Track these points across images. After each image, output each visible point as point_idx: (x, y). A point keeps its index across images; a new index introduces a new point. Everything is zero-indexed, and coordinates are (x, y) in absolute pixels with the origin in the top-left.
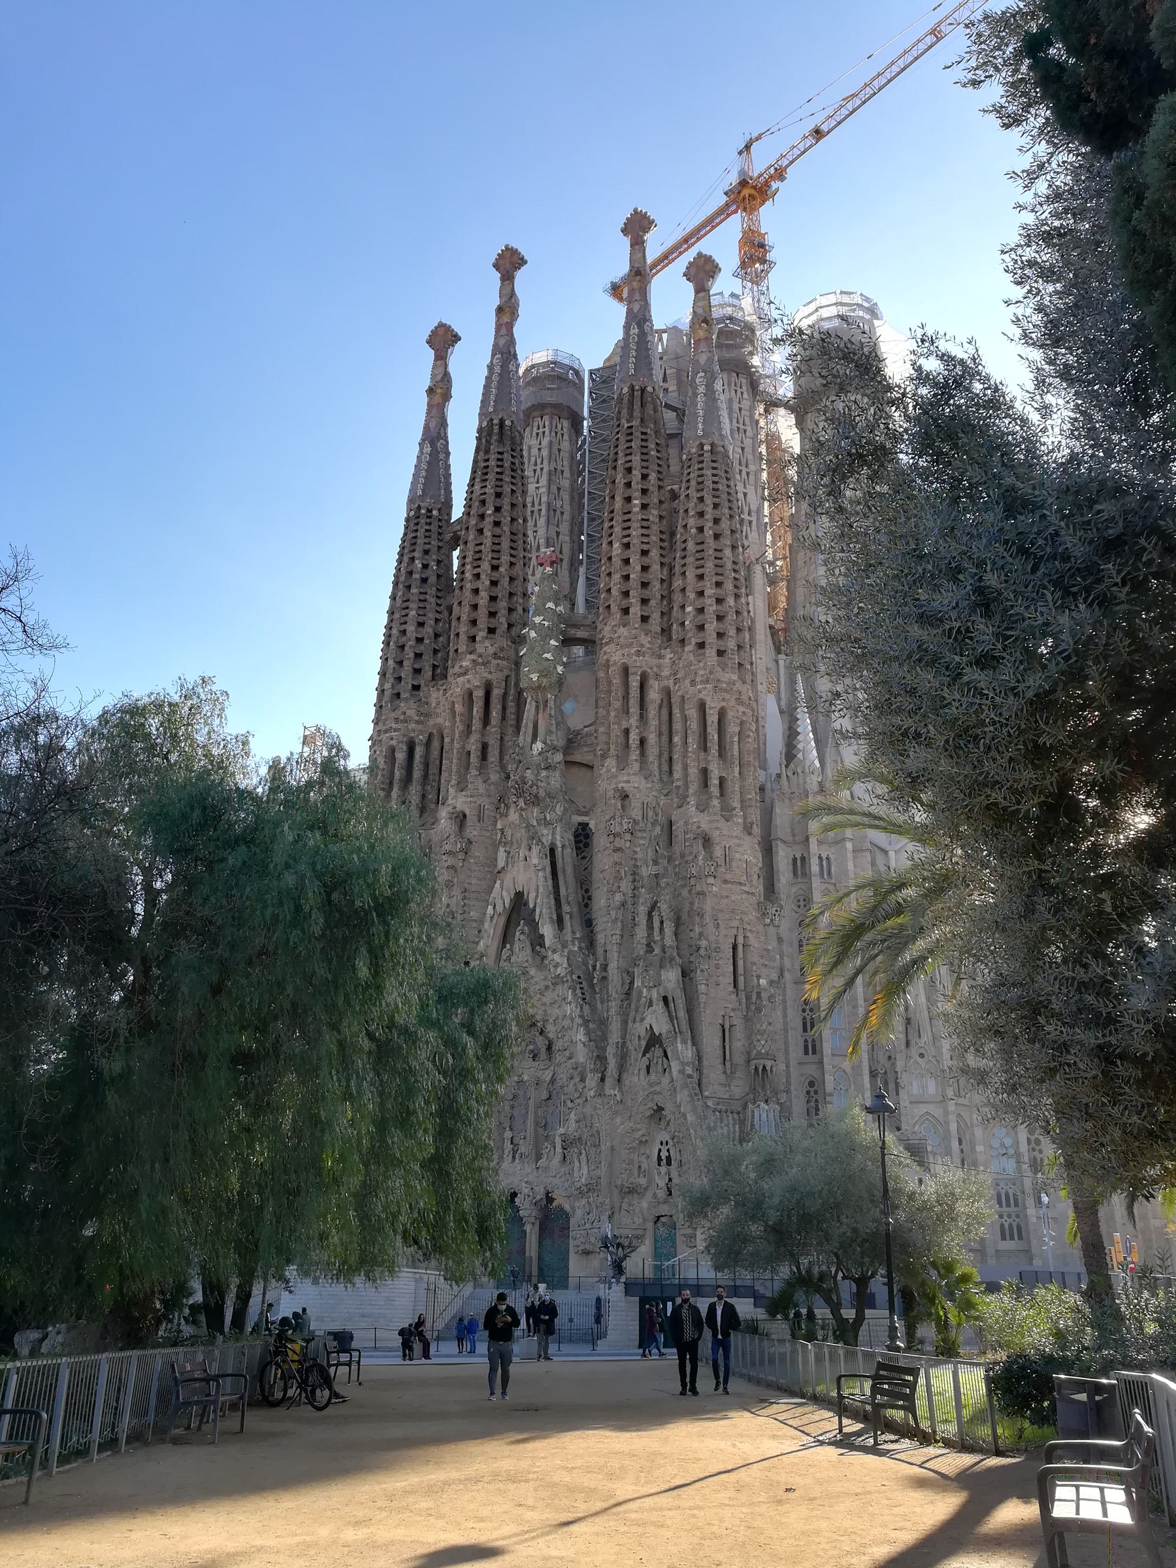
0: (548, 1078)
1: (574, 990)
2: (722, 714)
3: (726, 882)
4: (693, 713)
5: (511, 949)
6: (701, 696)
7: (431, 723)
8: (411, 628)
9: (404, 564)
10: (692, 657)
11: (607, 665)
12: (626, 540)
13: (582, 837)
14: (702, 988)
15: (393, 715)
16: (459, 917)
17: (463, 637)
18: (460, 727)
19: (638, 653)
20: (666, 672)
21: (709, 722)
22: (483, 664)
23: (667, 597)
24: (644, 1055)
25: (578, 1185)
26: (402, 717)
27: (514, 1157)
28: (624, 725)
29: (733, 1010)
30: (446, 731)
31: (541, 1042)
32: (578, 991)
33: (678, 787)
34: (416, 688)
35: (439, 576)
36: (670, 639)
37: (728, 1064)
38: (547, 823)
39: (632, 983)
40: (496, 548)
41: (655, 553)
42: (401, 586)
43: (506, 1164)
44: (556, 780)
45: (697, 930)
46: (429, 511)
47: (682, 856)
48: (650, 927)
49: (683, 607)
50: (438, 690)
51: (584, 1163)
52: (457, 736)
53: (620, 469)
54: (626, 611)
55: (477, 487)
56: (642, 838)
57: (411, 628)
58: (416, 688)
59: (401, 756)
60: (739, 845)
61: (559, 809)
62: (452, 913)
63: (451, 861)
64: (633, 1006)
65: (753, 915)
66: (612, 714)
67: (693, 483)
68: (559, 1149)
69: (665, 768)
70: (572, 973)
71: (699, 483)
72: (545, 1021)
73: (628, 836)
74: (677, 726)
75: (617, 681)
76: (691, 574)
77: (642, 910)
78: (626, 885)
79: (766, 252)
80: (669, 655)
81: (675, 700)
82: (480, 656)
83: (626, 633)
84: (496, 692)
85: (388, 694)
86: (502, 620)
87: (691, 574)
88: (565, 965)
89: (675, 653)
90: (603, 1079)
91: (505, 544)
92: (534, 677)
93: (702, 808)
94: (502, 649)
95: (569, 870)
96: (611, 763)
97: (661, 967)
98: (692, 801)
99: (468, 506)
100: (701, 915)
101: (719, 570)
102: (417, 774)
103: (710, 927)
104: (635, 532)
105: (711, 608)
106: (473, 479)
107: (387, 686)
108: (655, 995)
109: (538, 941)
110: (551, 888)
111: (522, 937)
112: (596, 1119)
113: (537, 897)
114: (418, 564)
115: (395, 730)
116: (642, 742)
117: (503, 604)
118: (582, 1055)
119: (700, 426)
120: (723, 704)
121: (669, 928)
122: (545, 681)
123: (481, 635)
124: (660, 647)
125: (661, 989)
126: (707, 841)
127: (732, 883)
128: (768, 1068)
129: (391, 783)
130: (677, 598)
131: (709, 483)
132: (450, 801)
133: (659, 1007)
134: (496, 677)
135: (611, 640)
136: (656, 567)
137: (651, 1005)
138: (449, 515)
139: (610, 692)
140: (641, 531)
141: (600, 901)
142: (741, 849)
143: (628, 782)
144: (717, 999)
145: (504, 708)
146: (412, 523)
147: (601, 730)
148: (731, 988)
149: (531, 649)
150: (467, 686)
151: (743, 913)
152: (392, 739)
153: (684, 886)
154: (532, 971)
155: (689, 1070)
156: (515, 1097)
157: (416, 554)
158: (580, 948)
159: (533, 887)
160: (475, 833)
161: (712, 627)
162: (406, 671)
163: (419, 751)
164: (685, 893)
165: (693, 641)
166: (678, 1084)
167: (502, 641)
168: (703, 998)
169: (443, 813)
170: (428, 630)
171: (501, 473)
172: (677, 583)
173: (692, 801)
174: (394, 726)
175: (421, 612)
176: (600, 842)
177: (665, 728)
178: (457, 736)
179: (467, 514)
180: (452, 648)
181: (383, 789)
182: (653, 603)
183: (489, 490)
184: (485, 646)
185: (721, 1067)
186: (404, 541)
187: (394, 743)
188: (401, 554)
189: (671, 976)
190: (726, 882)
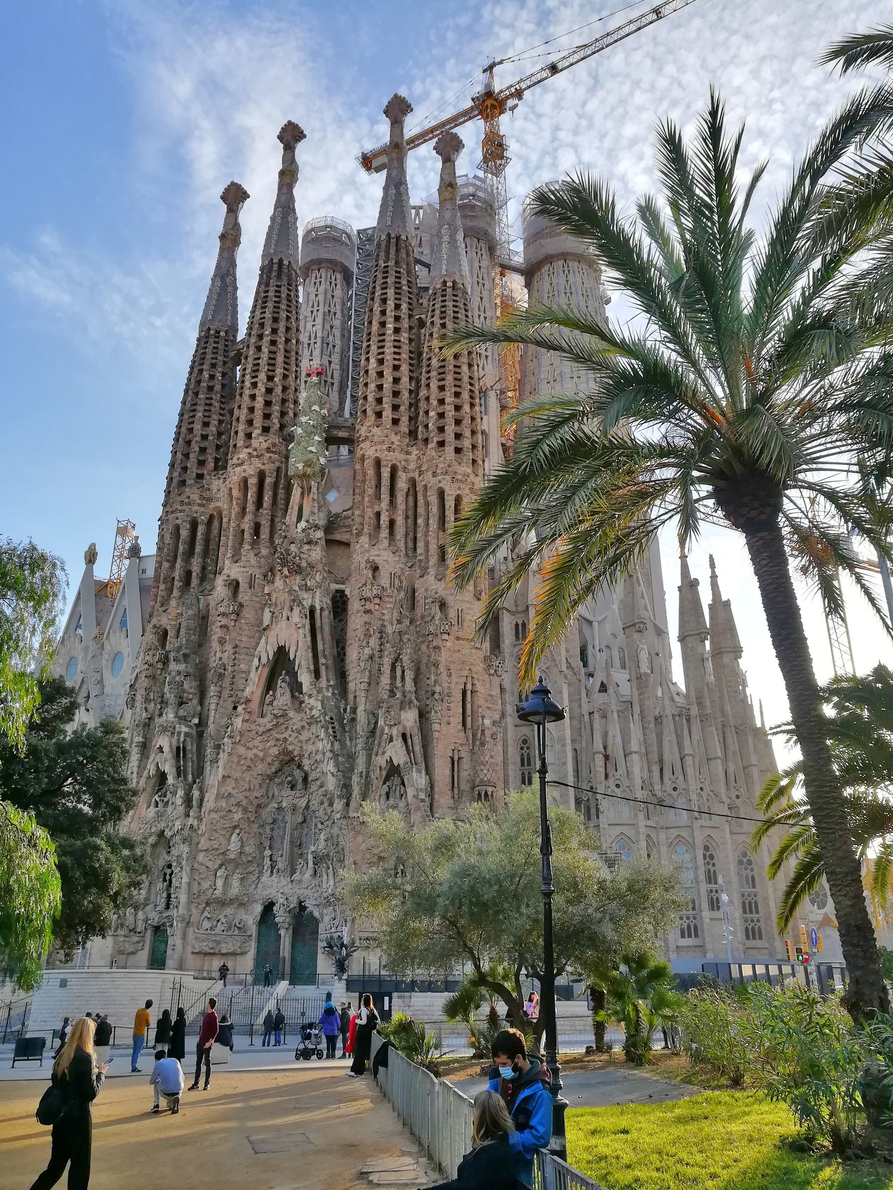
0: (304, 805)
1: (327, 729)
2: (458, 500)
3: (458, 638)
4: (433, 499)
5: (274, 695)
6: (441, 485)
7: (212, 505)
8: (197, 427)
9: (194, 375)
10: (434, 453)
11: (363, 458)
12: (380, 357)
13: (339, 603)
14: (436, 727)
15: (179, 498)
16: (230, 669)
17: (241, 434)
18: (236, 509)
19: (389, 449)
20: (412, 466)
21: (447, 507)
22: (257, 456)
23: (414, 405)
24: (384, 783)
25: (325, 895)
27: (272, 872)
28: (377, 509)
29: (461, 745)
30: (224, 513)
31: (298, 774)
32: (330, 731)
33: (420, 561)
35: (223, 386)
36: (416, 438)
37: (456, 790)
38: (308, 589)
39: (376, 723)
40: (272, 362)
41: (405, 368)
42: (190, 393)
43: (265, 878)
44: (317, 554)
45: (433, 678)
46: (218, 332)
47: (423, 617)
48: (393, 677)
49: (427, 413)
51: (331, 876)
52: (233, 516)
53: (377, 299)
54: (379, 415)
55: (258, 313)
56: (389, 602)
57: (197, 427)
58: (200, 476)
59: (184, 533)
60: (470, 609)
61: (318, 577)
62: (224, 665)
63: (224, 621)
64: (376, 742)
65: (480, 667)
66: (366, 499)
67: (437, 312)
68: (311, 864)
69: (411, 545)
70: (325, 714)
71: (442, 312)
72: (301, 756)
73: (377, 601)
74: (421, 510)
75: (371, 472)
76: (434, 385)
77: (387, 661)
78: (374, 642)
79: (504, 150)
80: (415, 452)
81: (419, 488)
82: (255, 450)
83: (379, 433)
84: (269, 480)
85: (175, 481)
86: (275, 421)
87: (434, 385)
88: (320, 708)
90: (348, 804)
91: (280, 359)
93: (440, 578)
94: (274, 445)
95: (327, 628)
96: (364, 540)
97: (401, 709)
98: (432, 571)
99: (250, 328)
100: (436, 665)
101: (458, 383)
102: (198, 548)
103: (444, 676)
104: (389, 350)
105: (450, 413)
106: (255, 306)
107: (176, 474)
108: (395, 731)
109: (296, 687)
110: (309, 643)
111: (283, 685)
112: (341, 839)
113: (296, 651)
114: (206, 375)
115: (181, 511)
116: (392, 523)
117: (276, 408)
118: (331, 784)
119: (444, 267)
120: (459, 492)
121: (409, 675)
122: (309, 470)
123: (256, 432)
124: (408, 445)
125: (400, 727)
126: (443, 605)
127: (463, 639)
128: (489, 793)
129: (175, 557)
130: (423, 405)
131: (450, 313)
132: (225, 571)
133: (398, 743)
134: (269, 468)
136: (405, 380)
137: (391, 740)
138: (235, 337)
139: (364, 481)
140: (393, 350)
141: (352, 654)
142: (471, 612)
143: (379, 555)
144: (448, 734)
145: (275, 495)
146: (203, 340)
147: (357, 512)
148: (460, 727)
151: (472, 664)
153: (423, 642)
154: (291, 714)
155: (422, 796)
156: (275, 821)
158: (333, 694)
159: (294, 642)
160: (246, 598)
161: (450, 429)
162: (192, 463)
163: (201, 529)
164: (424, 647)
165: (435, 440)
166: (412, 807)
167: (274, 438)
168: (436, 735)
169: (220, 581)
170: (213, 429)
171: (278, 302)
172: (423, 393)
173: (432, 571)
174: (180, 508)
175: (207, 414)
176: (354, 606)
177: (410, 513)
178: (233, 516)
179: (249, 335)
180: (232, 443)
181: (168, 561)
182: (402, 408)
183: (268, 315)
184: (259, 442)
185: (450, 793)
186: (195, 356)
187: (179, 522)
188: (192, 368)
189: (410, 718)
190: (458, 638)
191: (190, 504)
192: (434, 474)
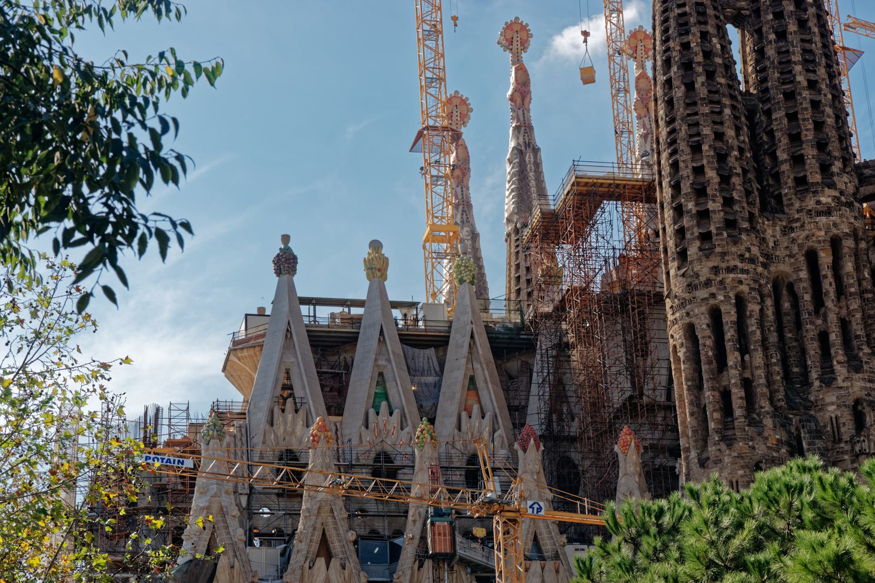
8: (731, 133)
26: (747, 255)
34: (751, 217)
50: (774, 225)
115: (743, 271)
150: (835, 231)
152: (740, 282)
157: (711, 29)
174: (740, 265)
187: (744, 288)
191: (752, 261)
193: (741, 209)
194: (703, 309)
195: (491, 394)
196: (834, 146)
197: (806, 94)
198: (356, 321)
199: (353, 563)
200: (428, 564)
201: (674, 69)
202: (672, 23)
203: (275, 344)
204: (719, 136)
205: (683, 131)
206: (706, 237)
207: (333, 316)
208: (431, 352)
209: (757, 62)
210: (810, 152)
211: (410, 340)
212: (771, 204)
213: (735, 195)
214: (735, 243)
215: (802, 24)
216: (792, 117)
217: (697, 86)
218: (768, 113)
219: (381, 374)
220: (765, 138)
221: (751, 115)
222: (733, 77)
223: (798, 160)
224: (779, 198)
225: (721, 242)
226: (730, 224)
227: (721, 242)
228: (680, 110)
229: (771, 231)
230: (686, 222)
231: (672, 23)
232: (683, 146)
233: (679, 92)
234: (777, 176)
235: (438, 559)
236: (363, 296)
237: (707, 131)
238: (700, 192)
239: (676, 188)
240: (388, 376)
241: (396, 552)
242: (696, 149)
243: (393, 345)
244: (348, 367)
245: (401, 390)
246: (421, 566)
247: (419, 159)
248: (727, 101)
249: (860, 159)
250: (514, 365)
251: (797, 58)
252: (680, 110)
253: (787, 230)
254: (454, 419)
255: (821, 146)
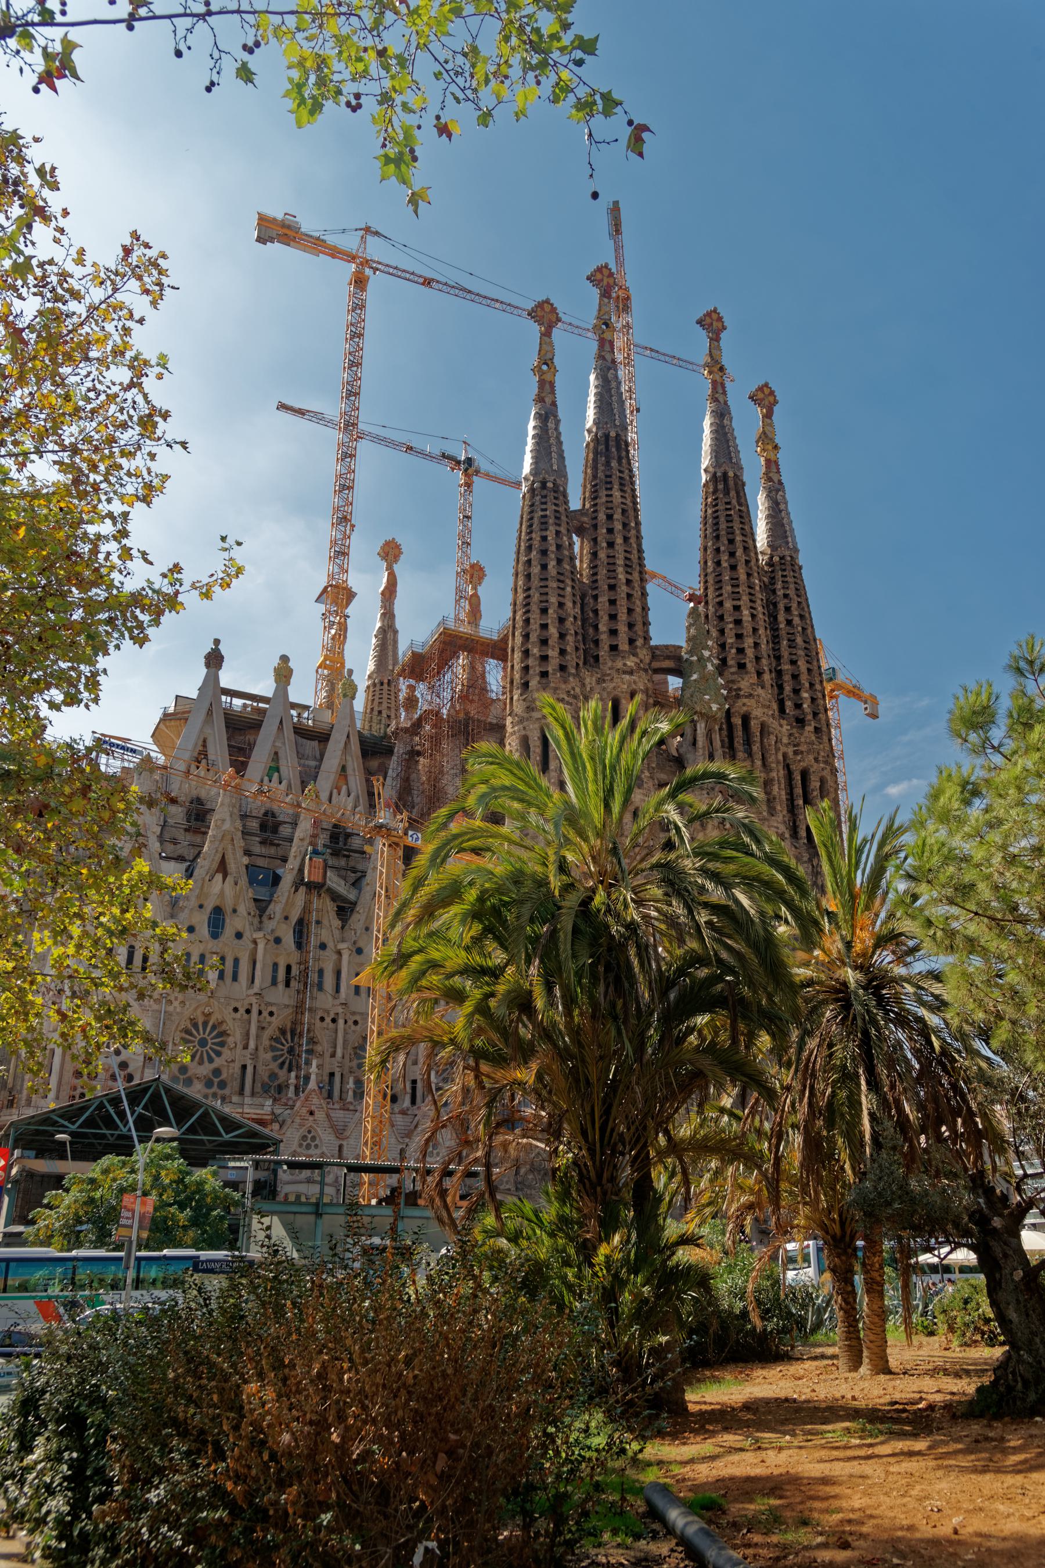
8: (569, 604)
11: (746, 719)
20: (785, 740)
67: (792, 586)
89: (792, 727)
92: (715, 707)
130: (787, 677)
135: (750, 695)
149: (704, 678)
157: (563, 530)
183: (628, 502)
191: (575, 697)
192: (816, 760)
193: (572, 659)
194: (537, 726)
195: (356, 781)
196: (639, 628)
197: (624, 588)
198: (264, 712)
199: (244, 880)
200: (302, 890)
201: (534, 553)
202: (536, 521)
203: (197, 720)
204: (561, 605)
205: (536, 597)
206: (544, 674)
207: (245, 706)
208: (315, 743)
209: (591, 561)
210: (622, 628)
211: (301, 731)
212: (592, 660)
213: (569, 649)
214: (565, 682)
215: (626, 539)
216: (612, 602)
217: (550, 567)
218: (595, 598)
219: (276, 753)
220: (591, 615)
221: (583, 597)
222: (574, 566)
223: (613, 632)
224: (597, 658)
225: (555, 677)
226: (563, 668)
227: (555, 677)
228: (535, 582)
229: (590, 680)
230: (531, 662)
231: (536, 521)
232: (535, 608)
233: (536, 570)
234: (597, 642)
235: (311, 886)
236: (270, 695)
237: (553, 600)
238: (544, 642)
239: (526, 637)
240: (281, 754)
241: (276, 880)
242: (544, 611)
243: (289, 733)
244: (251, 746)
245: (290, 766)
246: (296, 890)
247: (322, 608)
248: (569, 582)
249: (652, 643)
250: (374, 764)
251: (620, 562)
252: (535, 582)
253: (600, 681)
254: (328, 794)
255: (631, 626)
